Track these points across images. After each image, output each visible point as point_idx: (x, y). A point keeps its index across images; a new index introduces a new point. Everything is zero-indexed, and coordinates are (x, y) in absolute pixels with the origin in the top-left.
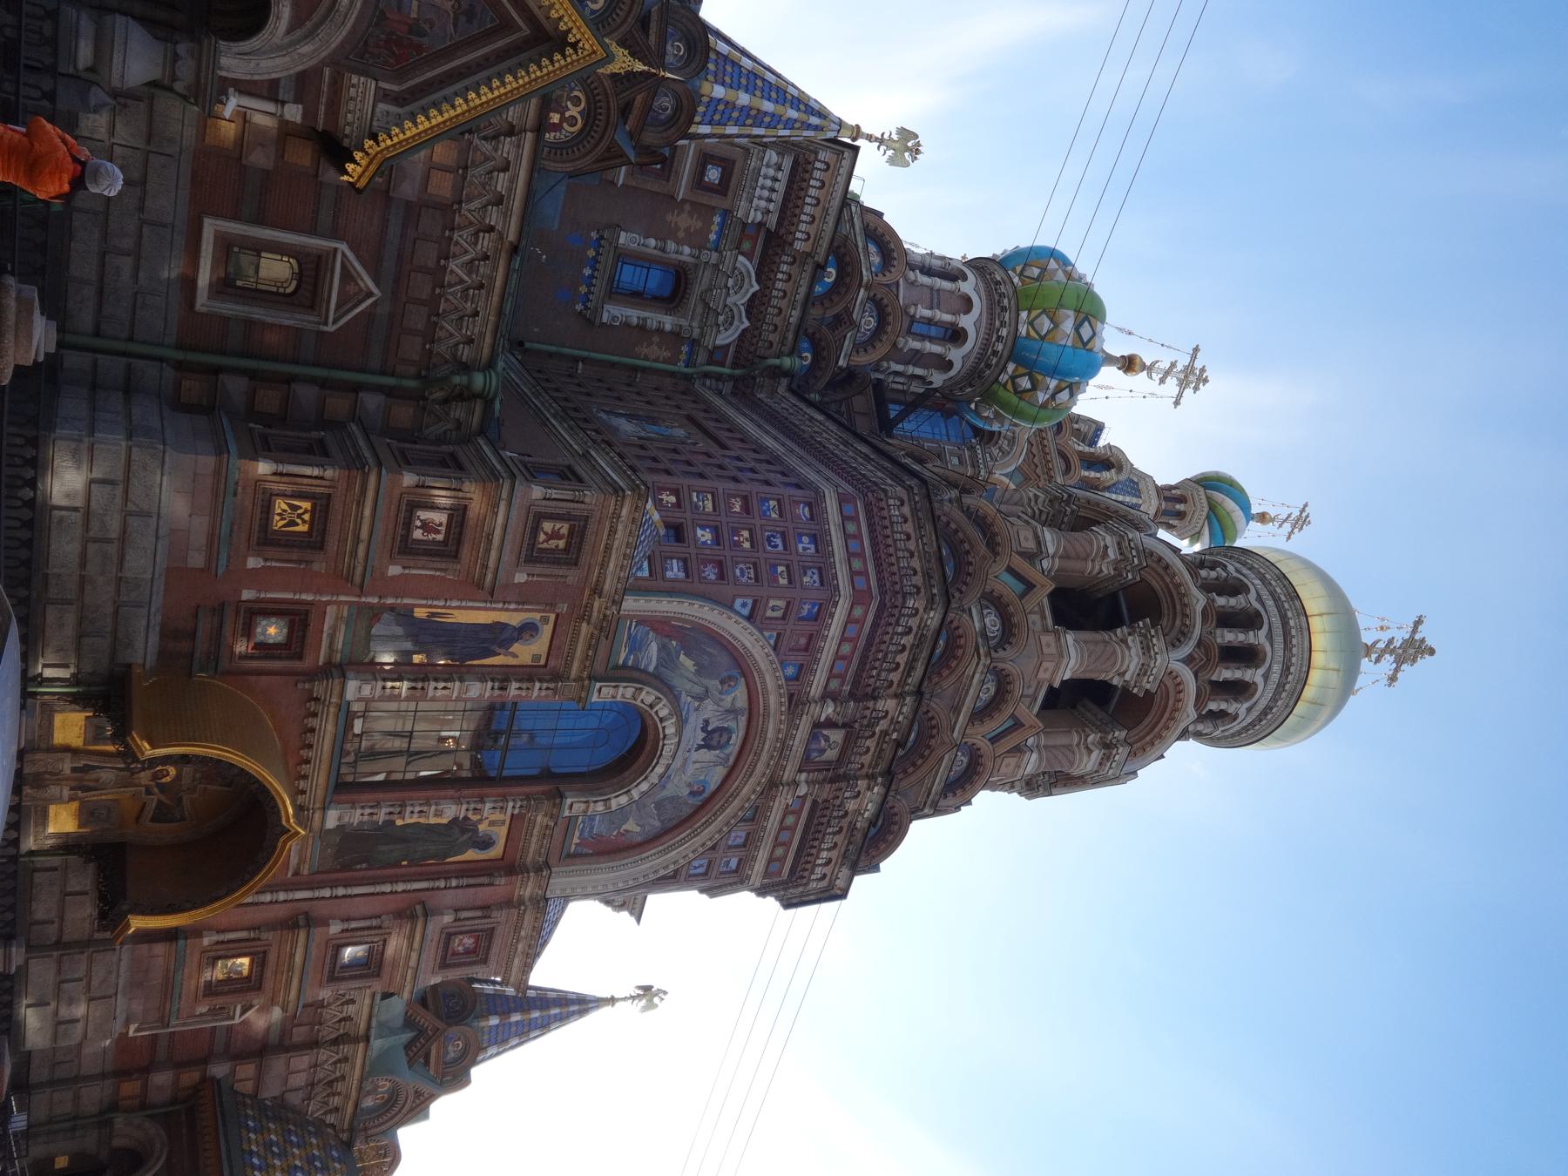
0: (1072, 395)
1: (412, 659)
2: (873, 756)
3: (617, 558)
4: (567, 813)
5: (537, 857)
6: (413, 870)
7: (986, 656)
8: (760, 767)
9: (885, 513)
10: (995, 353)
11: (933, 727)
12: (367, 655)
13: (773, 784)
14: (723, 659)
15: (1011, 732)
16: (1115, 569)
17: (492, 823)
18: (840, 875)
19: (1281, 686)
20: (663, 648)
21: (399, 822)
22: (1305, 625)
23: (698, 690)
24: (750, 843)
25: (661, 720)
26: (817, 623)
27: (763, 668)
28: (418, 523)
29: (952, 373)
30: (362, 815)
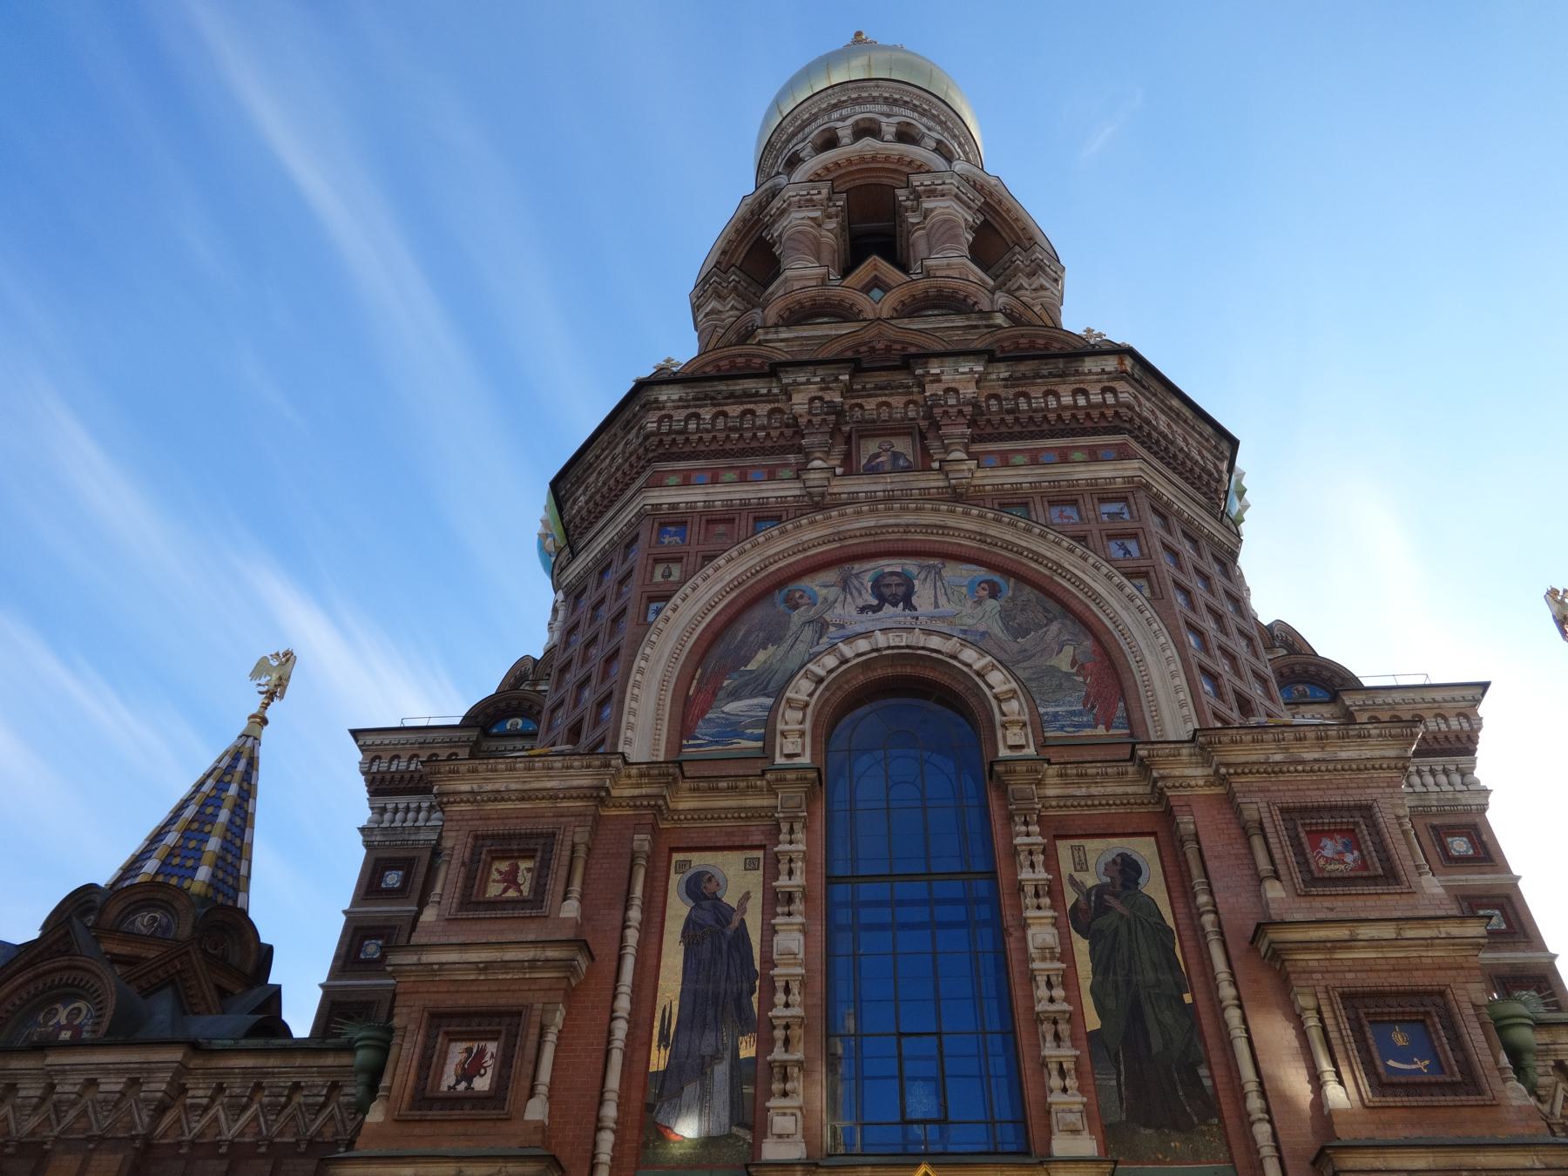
1: (748, 1060)
2: (891, 395)
3: (538, 778)
4: (1031, 751)
5: (1130, 777)
6: (1197, 981)
7: (755, 337)
12: (737, 1138)
14: (758, 614)
17: (1082, 866)
20: (735, 695)
21: (1093, 1022)
23: (808, 634)
26: (689, 519)
27: (758, 559)
28: (463, 1085)
30: (1065, 1090)
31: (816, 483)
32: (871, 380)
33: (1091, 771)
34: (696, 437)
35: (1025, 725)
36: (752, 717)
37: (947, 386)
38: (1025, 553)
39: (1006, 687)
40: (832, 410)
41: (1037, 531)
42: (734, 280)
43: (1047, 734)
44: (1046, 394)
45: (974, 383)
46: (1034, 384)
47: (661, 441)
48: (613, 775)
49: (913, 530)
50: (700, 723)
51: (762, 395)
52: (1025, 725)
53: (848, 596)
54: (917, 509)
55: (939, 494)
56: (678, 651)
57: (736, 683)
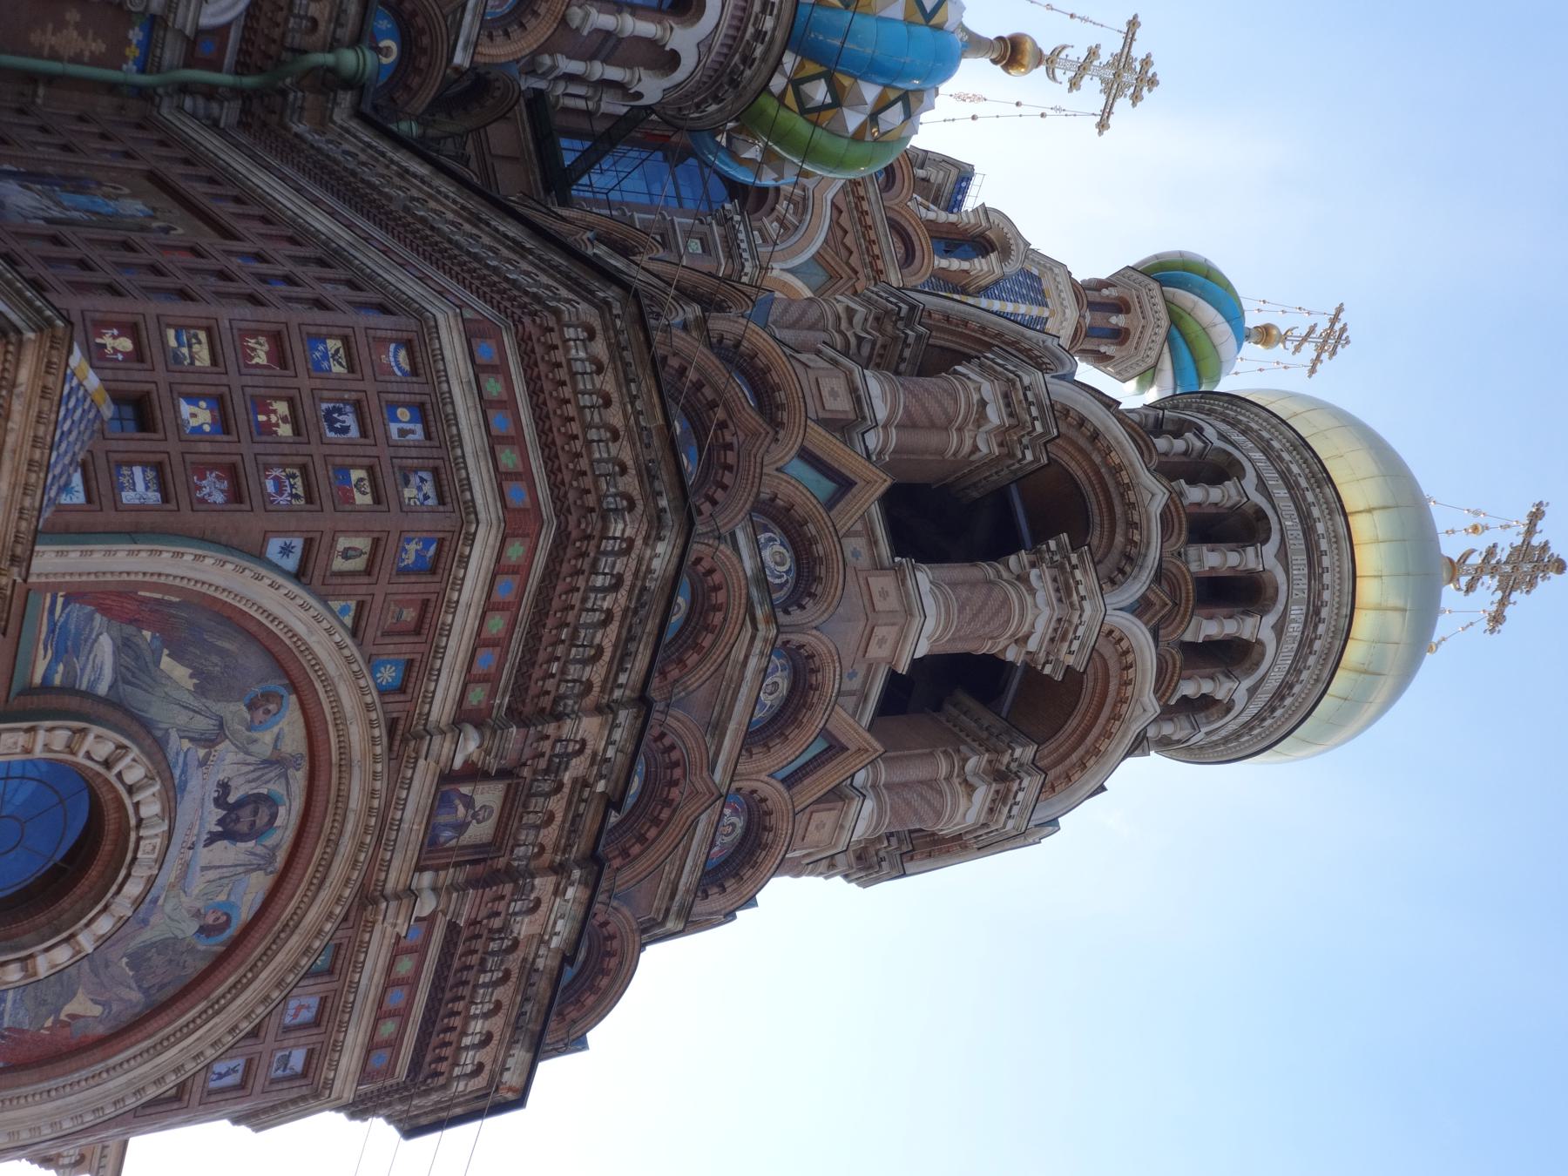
0: (909, 114)
2: (562, 828)
3: (16, 470)
7: (767, 623)
8: (338, 869)
9: (558, 356)
10: (759, 35)
11: (676, 764)
13: (367, 898)
14: (253, 662)
15: (824, 764)
16: (1001, 445)
18: (510, 1063)
19: (1305, 644)
20: (124, 646)
22: (1342, 531)
23: (202, 724)
24: (326, 1018)
25: (131, 790)
26: (437, 578)
29: (680, 75)
34: (581, 583)
36: (83, 670)
40: (554, 768)
49: (328, 850)
50: (89, 608)
51: (617, 675)
53: (251, 768)
54: (356, 861)
57: (144, 646)
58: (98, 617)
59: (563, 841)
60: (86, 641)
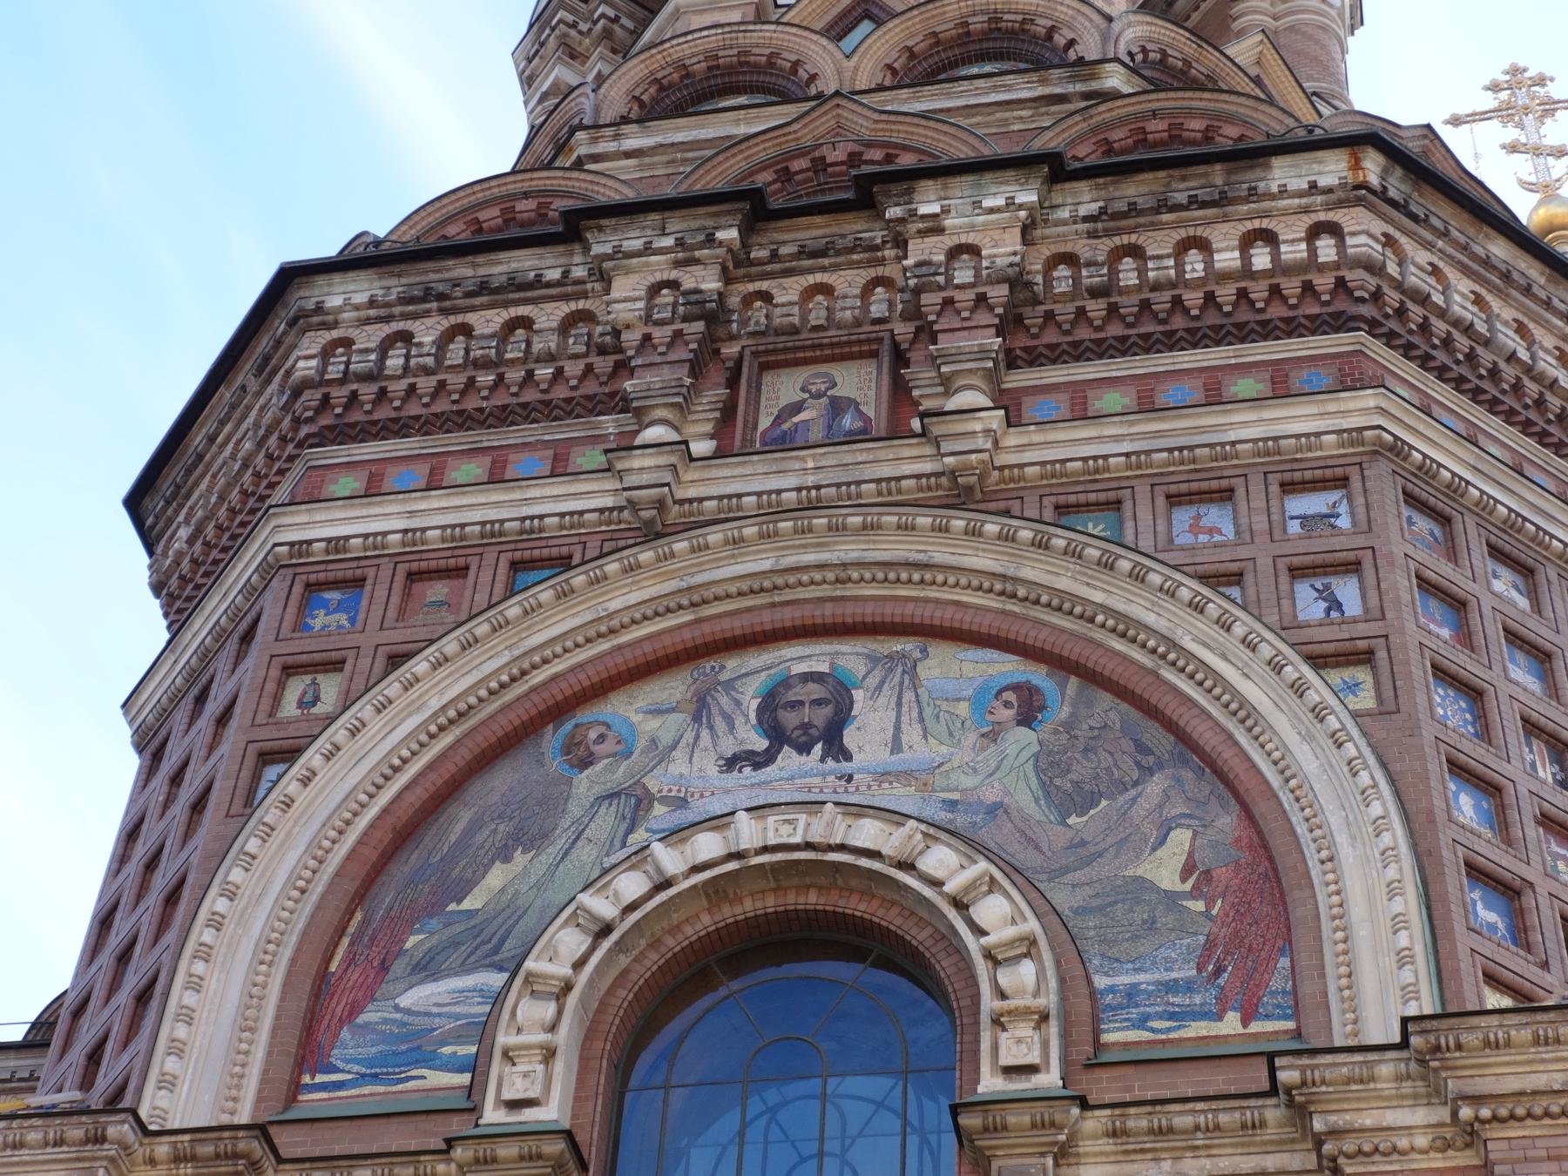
2: (836, 267)
4: (1050, 1079)
5: (1271, 1133)
7: (572, 151)
14: (502, 781)
20: (427, 969)
23: (605, 822)
26: (371, 573)
27: (506, 657)
31: (645, 479)
32: (789, 238)
33: (1183, 1121)
34: (403, 385)
35: (1044, 1017)
36: (458, 1017)
37: (955, 240)
38: (1100, 618)
39: (1010, 932)
40: (695, 309)
41: (1124, 565)
42: (603, 16)
43: (1108, 1038)
44: (1183, 247)
45: (1017, 232)
46: (1156, 226)
47: (326, 398)
48: (112, 1160)
49: (855, 575)
50: (345, 1034)
51: (549, 285)
52: (1044, 1017)
53: (705, 733)
54: (864, 527)
55: (920, 489)
56: (308, 874)
57: (435, 940)
58: (362, 1018)
59: (855, 257)
60: (405, 1024)
